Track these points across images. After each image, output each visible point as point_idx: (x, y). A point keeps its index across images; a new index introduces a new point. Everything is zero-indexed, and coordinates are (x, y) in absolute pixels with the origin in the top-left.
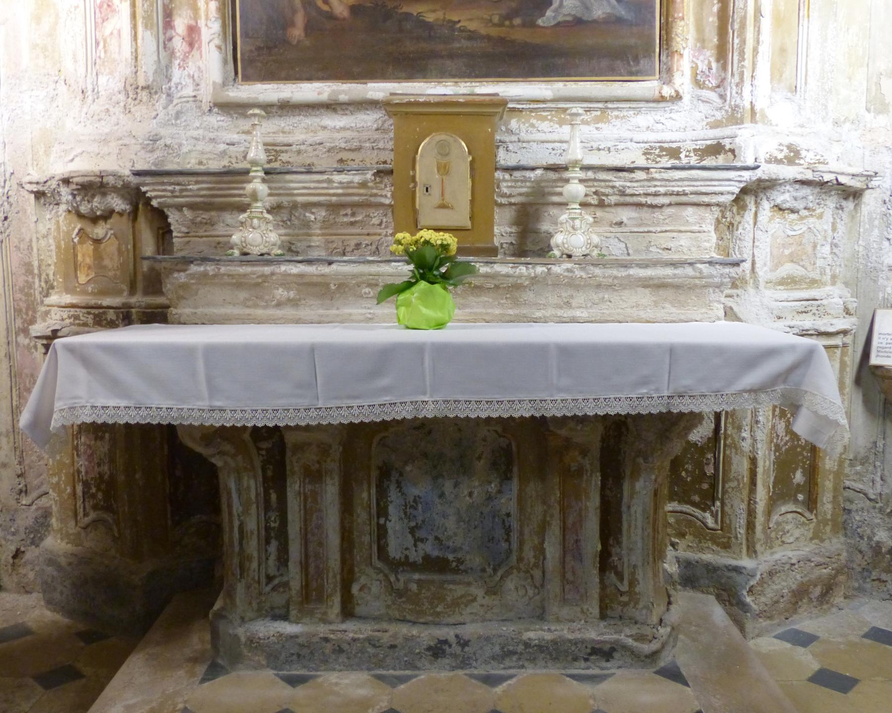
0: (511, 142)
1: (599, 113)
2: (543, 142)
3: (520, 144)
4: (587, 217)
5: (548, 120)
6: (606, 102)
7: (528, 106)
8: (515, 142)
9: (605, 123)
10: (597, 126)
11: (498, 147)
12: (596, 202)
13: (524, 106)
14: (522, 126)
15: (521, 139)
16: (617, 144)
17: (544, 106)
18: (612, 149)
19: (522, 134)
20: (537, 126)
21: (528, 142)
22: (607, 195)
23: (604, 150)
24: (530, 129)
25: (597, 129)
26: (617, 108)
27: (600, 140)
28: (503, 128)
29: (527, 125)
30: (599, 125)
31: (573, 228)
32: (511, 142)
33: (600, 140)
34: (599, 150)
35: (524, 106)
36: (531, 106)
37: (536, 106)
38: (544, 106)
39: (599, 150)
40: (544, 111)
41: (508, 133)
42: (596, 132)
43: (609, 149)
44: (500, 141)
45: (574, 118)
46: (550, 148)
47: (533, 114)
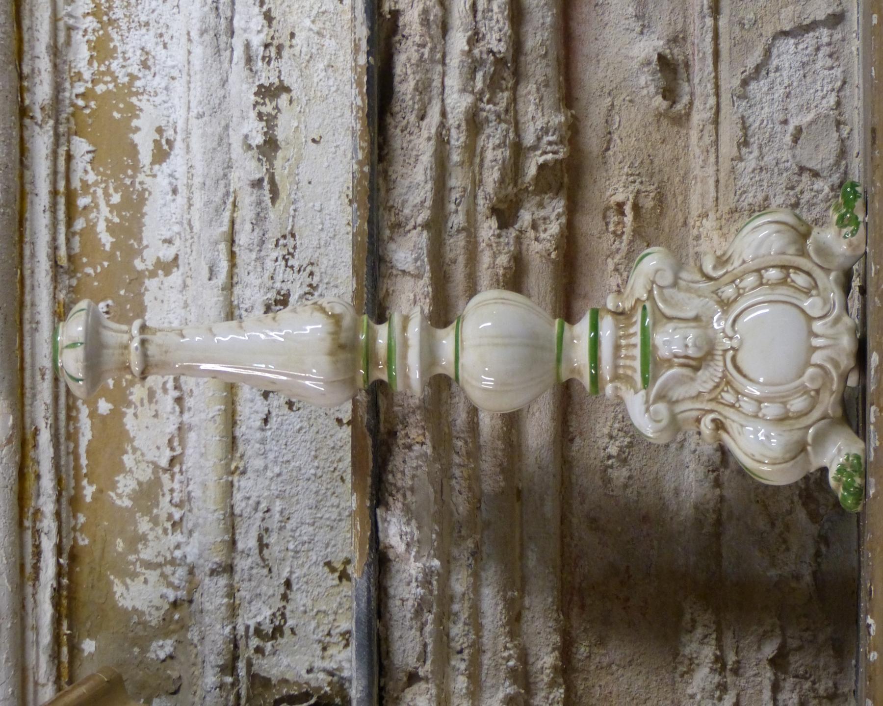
0: (233, 611)
1: (81, 146)
2: (232, 442)
3: (242, 564)
4: (638, 287)
5: (117, 415)
6: (23, 112)
7: (48, 523)
8: (231, 593)
9: (133, 112)
10: (145, 155)
11: (259, 682)
12: (557, 207)
13: (48, 545)
14: (147, 554)
15: (217, 558)
16: (239, 53)
17: (45, 437)
18: (267, 76)
19: (191, 551)
20: (145, 474)
21: (231, 521)
22: (518, 151)
23: (269, 121)
24: (164, 506)
25: (161, 154)
26: (55, 51)
27: (222, 140)
28: (162, 648)
29: (144, 525)
30: (144, 142)
31: (695, 364)
32: (233, 611)
33: (222, 140)
34: (270, 146)
35: (48, 545)
36: (48, 506)
37: (47, 483)
38: (45, 437)
39: (270, 146)
40: (73, 437)
41: (183, 626)
42: (177, 162)
43: (268, 92)
44: (229, 668)
45: (111, 358)
46: (261, 406)
47: (89, 491)
